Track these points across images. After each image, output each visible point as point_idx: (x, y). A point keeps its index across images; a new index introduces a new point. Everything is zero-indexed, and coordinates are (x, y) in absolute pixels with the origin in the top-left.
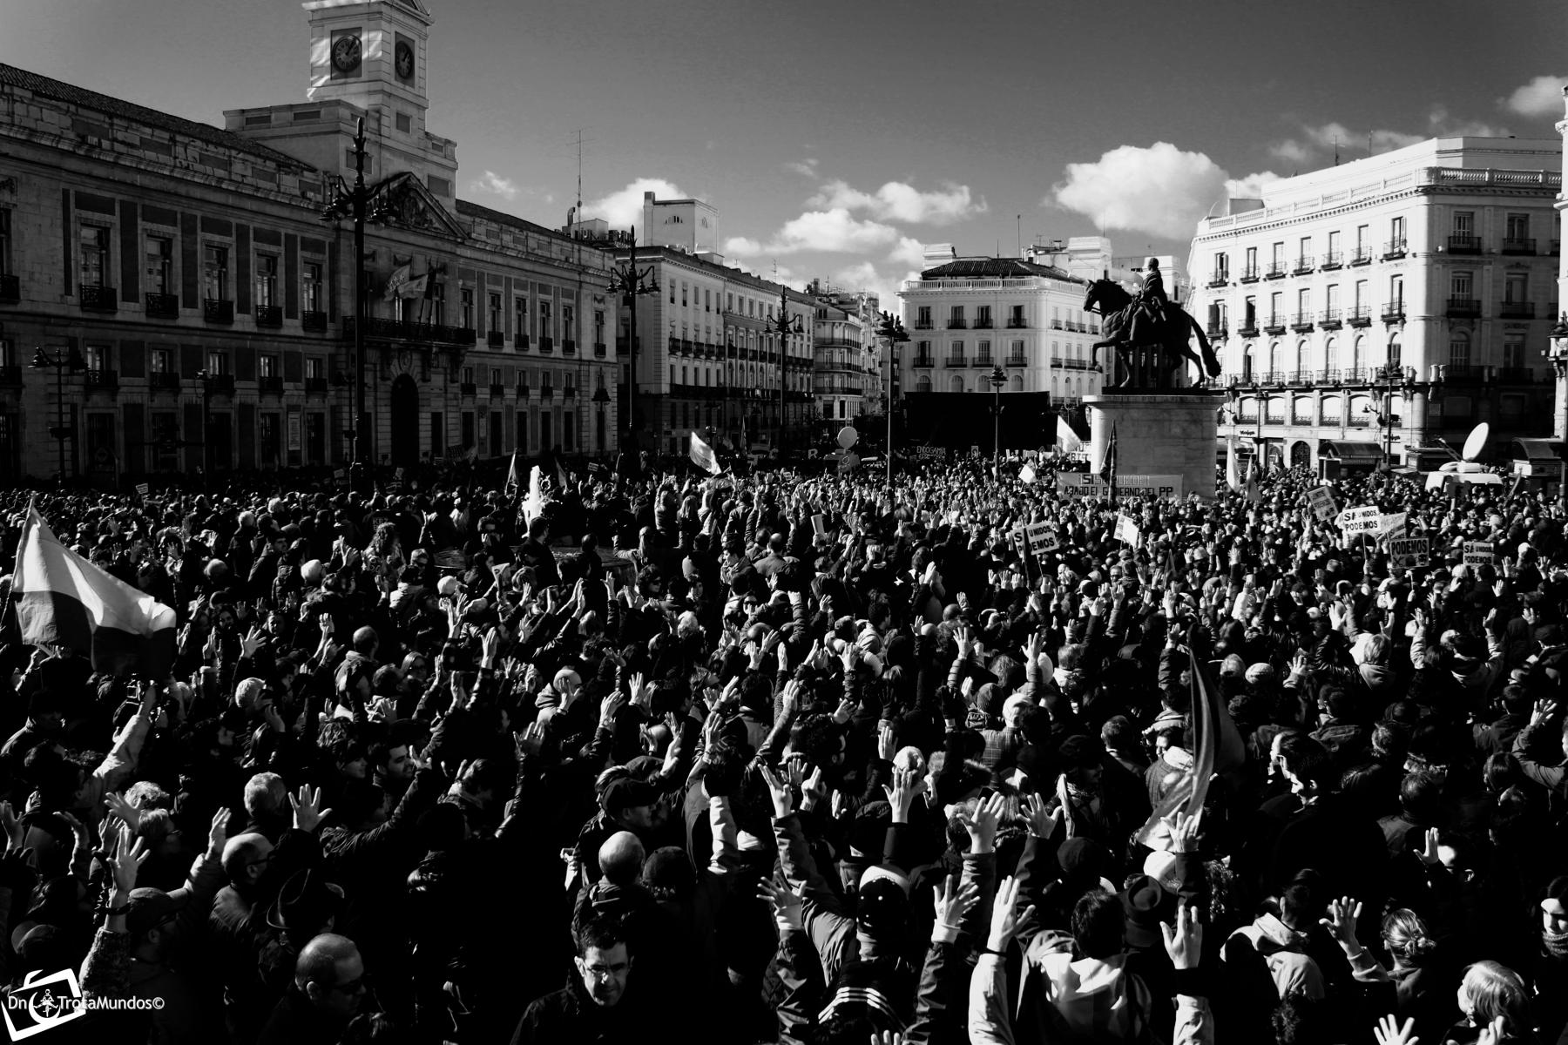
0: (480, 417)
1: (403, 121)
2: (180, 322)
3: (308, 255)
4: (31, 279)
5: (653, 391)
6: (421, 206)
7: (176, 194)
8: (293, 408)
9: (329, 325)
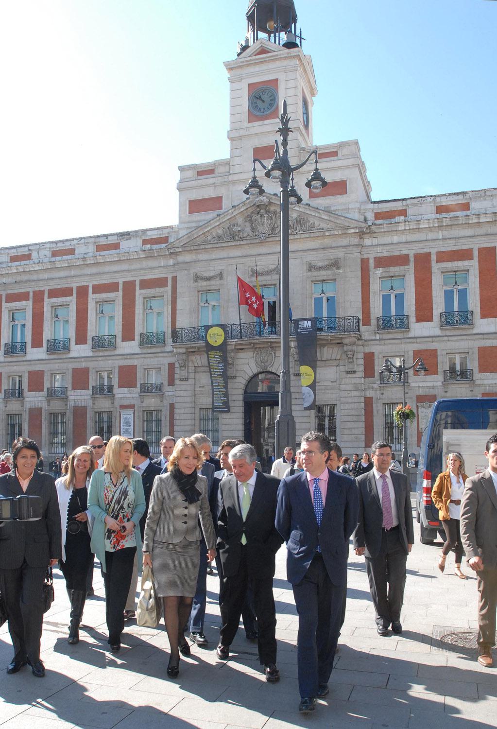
2: (29, 357)
7: (29, 281)
8: (123, 407)
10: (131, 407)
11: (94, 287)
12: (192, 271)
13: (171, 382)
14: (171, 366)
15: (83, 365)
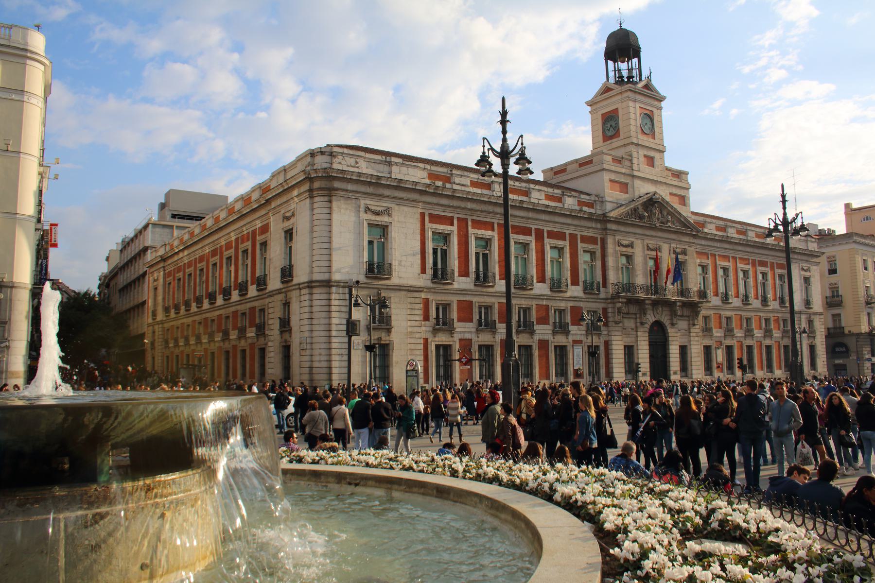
0: (717, 348)
1: (651, 161)
3: (585, 246)
4: (400, 264)
5: (855, 330)
6: (665, 213)
8: (576, 342)
9: (602, 289)
10: (580, 342)
11: (548, 232)
12: (617, 238)
13: (606, 324)
14: (605, 310)
15: (468, 298)
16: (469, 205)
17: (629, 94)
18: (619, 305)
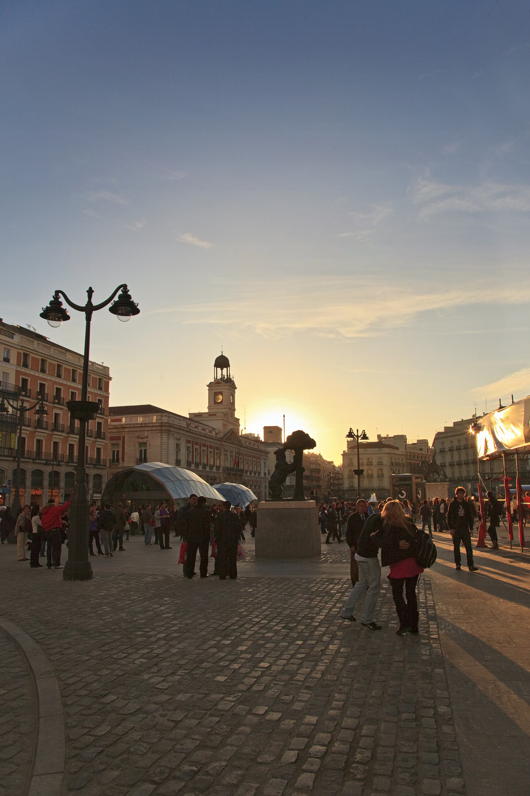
16: (194, 436)
17: (228, 387)
18: (225, 475)
